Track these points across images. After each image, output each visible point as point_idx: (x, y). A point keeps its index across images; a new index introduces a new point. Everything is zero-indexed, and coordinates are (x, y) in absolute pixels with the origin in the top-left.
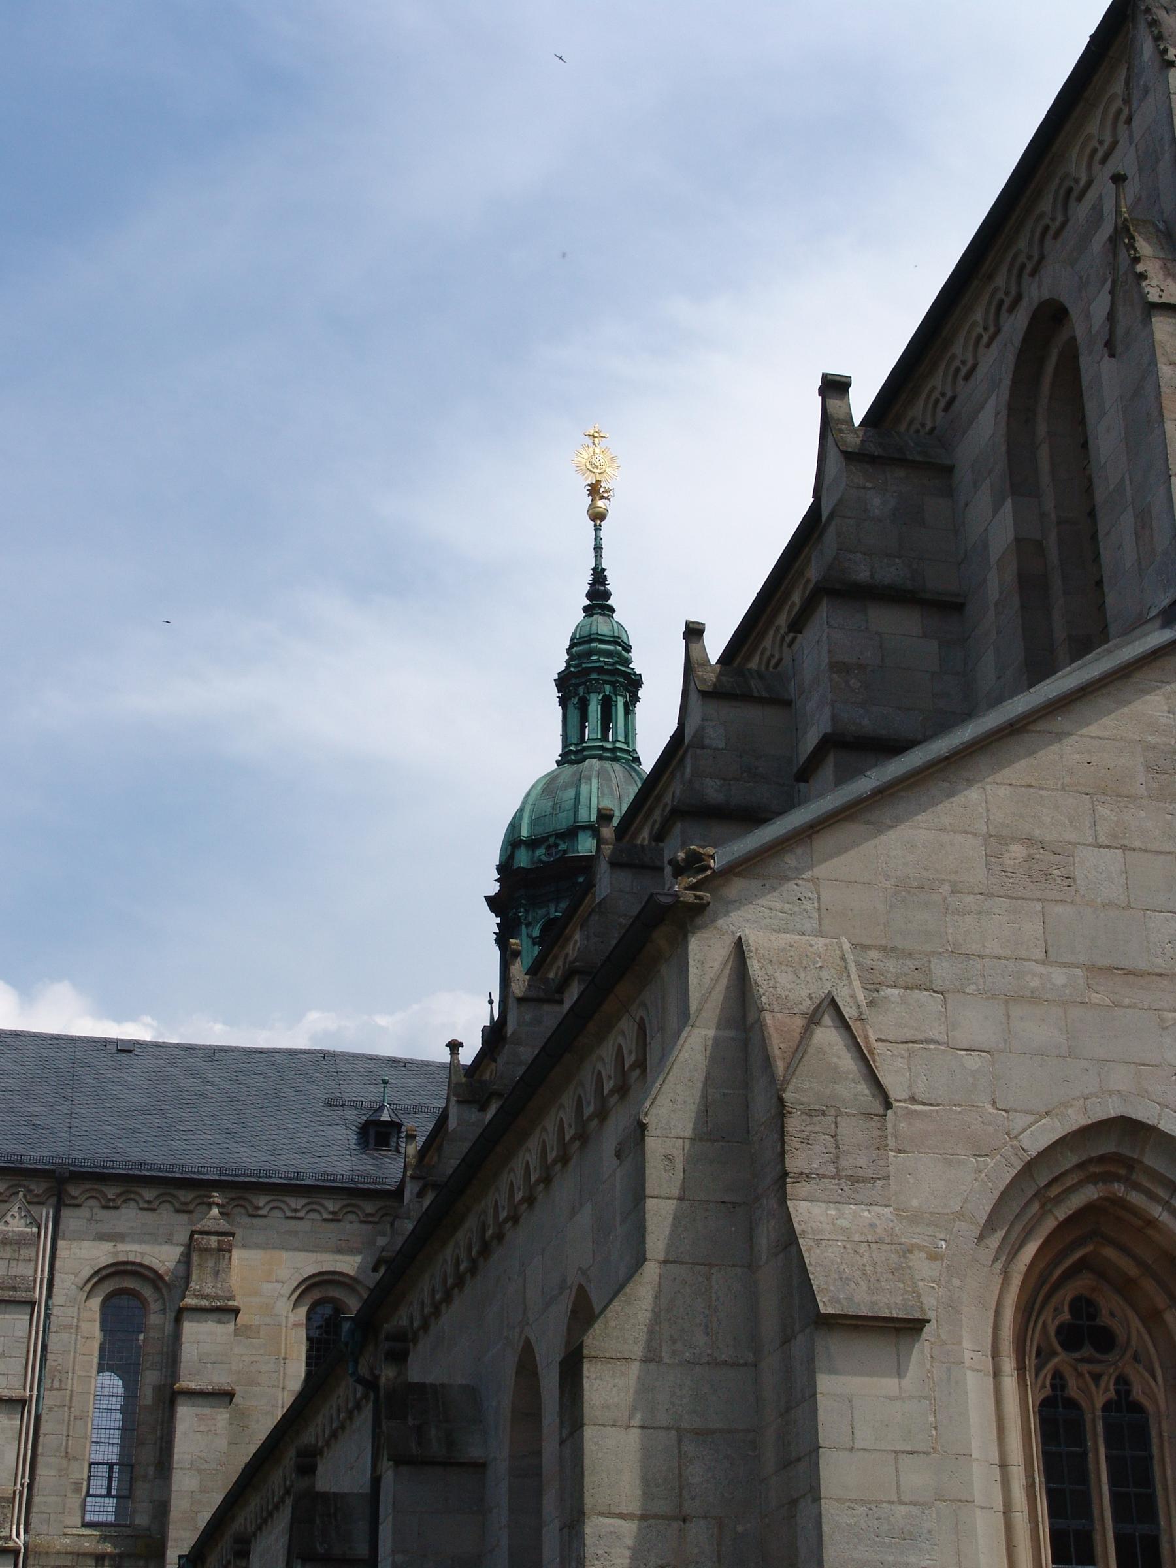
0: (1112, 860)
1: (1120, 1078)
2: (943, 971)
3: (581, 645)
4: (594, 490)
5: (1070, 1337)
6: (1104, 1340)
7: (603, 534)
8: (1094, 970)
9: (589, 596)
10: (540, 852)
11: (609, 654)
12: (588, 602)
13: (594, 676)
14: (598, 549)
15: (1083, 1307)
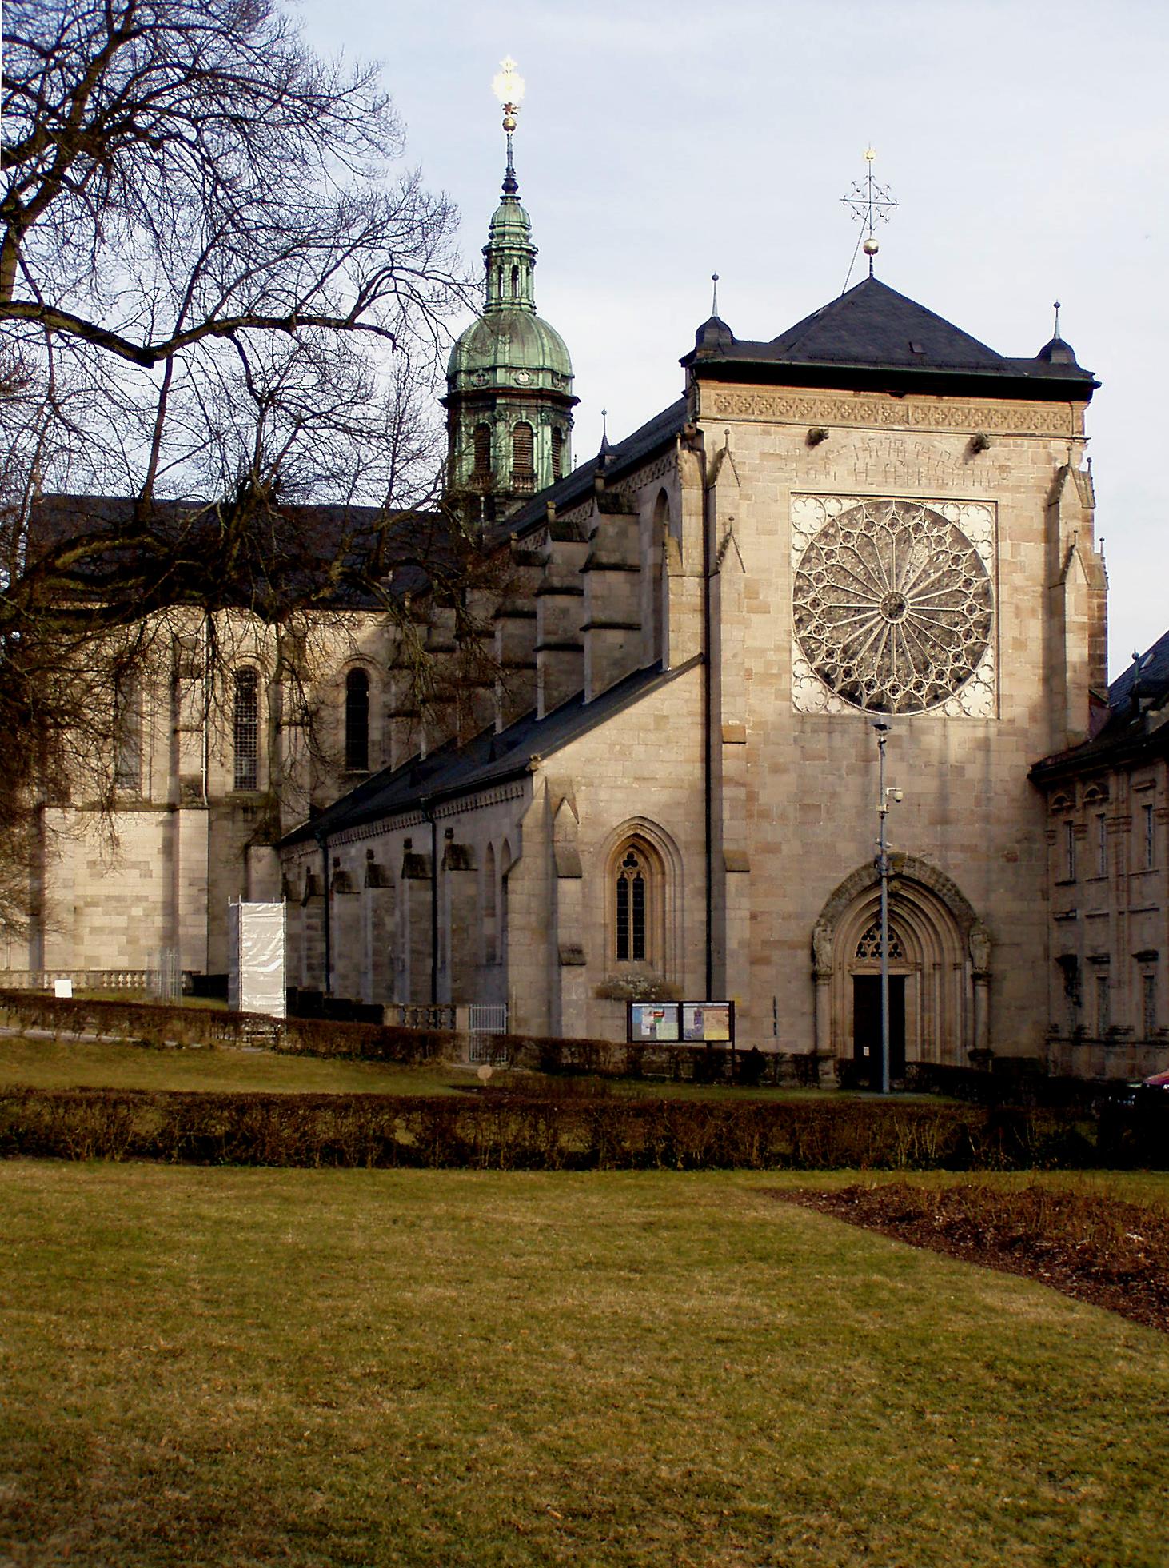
0: (642, 748)
1: (639, 807)
2: (596, 782)
3: (497, 229)
4: (508, 108)
5: (626, 863)
6: (635, 864)
7: (512, 141)
8: (636, 779)
9: (506, 188)
10: (474, 378)
11: (518, 235)
12: (503, 193)
13: (507, 252)
14: (510, 153)
15: (630, 856)
